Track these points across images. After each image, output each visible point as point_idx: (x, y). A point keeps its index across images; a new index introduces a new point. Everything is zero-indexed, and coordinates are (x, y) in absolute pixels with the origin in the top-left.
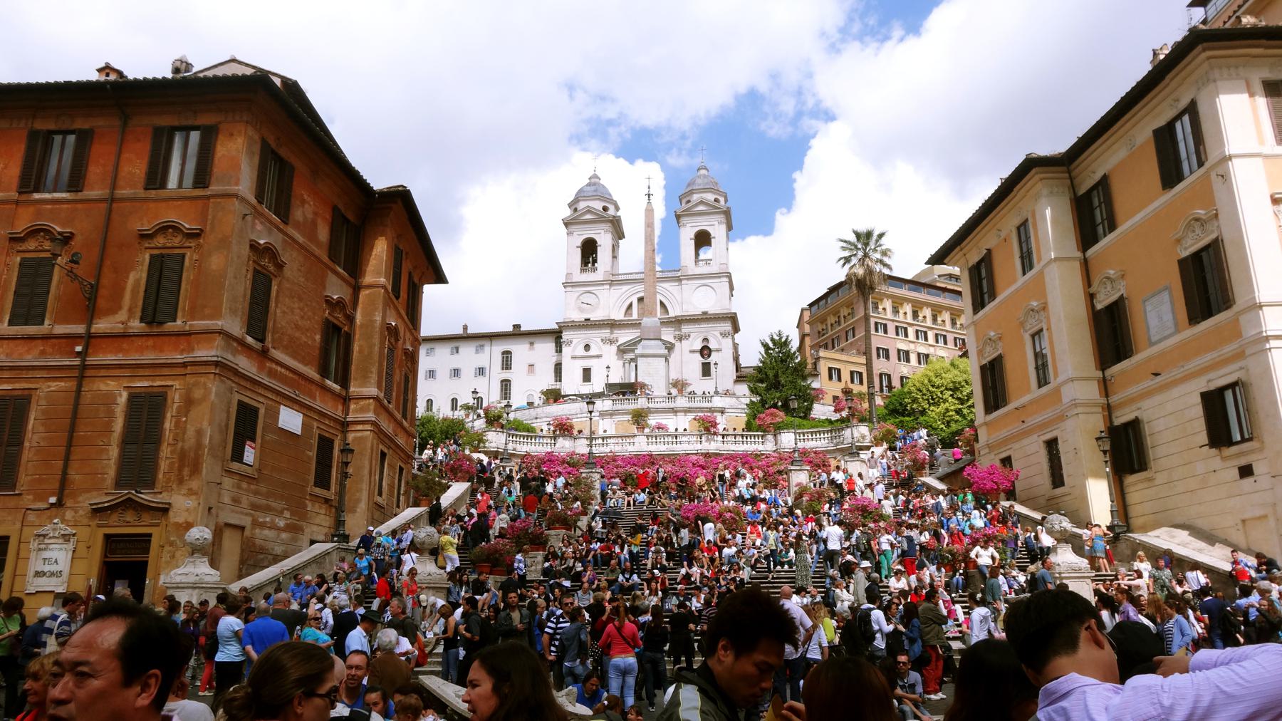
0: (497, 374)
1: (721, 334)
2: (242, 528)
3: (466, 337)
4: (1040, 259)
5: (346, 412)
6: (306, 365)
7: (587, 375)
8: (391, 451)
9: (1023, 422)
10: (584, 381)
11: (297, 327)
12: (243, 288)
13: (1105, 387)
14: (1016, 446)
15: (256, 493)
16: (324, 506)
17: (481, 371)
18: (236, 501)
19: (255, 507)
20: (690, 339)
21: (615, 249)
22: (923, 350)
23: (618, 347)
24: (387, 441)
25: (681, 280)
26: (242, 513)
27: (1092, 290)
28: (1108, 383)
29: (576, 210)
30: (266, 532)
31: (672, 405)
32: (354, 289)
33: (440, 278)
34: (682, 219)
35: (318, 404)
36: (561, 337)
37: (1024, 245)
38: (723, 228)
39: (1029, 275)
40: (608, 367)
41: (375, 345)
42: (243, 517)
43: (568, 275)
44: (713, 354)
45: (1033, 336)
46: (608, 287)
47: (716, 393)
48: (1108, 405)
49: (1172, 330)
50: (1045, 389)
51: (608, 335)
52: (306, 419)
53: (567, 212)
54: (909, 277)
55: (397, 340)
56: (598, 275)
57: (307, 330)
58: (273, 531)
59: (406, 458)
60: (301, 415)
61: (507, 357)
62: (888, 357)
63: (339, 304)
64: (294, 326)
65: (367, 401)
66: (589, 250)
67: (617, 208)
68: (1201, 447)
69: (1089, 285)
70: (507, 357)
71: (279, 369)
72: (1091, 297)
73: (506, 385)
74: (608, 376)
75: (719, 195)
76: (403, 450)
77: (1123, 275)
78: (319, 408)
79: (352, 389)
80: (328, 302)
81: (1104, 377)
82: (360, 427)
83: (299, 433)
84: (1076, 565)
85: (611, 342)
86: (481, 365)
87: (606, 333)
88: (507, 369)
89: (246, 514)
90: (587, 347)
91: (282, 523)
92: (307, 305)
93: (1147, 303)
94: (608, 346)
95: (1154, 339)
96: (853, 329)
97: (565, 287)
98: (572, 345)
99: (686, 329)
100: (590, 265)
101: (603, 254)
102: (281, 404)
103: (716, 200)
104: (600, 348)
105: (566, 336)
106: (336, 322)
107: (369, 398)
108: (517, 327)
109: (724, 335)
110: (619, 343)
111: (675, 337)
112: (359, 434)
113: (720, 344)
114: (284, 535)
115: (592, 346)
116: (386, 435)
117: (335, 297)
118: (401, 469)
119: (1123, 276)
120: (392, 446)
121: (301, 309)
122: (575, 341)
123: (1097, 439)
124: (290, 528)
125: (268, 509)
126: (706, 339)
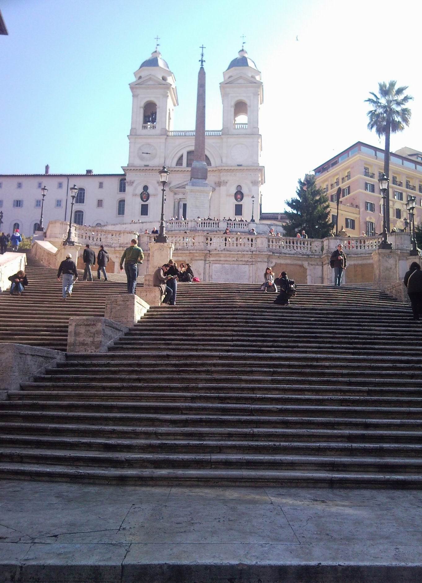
7: (144, 210)
10: (142, 214)
20: (228, 185)
23: (170, 188)
25: (222, 139)
29: (140, 78)
36: (125, 179)
43: (132, 130)
44: (244, 198)
53: (133, 79)
56: (157, 131)
70: (81, 193)
88: (80, 202)
90: (146, 188)
96: (349, 187)
97: (129, 139)
98: (134, 185)
104: (156, 189)
108: (89, 171)
113: (250, 191)
126: (239, 186)
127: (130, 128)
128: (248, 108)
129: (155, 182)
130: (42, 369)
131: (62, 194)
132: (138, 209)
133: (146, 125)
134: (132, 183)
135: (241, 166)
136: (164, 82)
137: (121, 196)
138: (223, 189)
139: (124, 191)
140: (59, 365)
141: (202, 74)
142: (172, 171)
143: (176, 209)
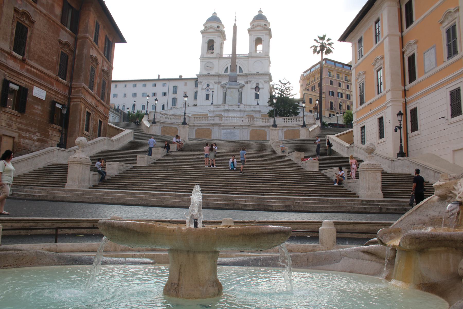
0: (171, 95)
1: (264, 81)
2: (14, 138)
3: (159, 80)
4: (382, 36)
5: (70, 92)
6: (48, 69)
8: (94, 113)
9: (371, 110)
10: (206, 99)
11: (43, 52)
12: (10, 29)
13: (405, 93)
14: (367, 121)
15: (20, 123)
16: (59, 133)
17: (165, 94)
18: (9, 125)
19: (19, 129)
20: (251, 83)
21: (222, 44)
22: (348, 93)
23: (221, 85)
24: (91, 108)
25: (249, 58)
26: (13, 131)
27: (403, 50)
28: (407, 92)
29: (206, 27)
30: (27, 141)
31: (239, 109)
32: (75, 39)
33: (122, 40)
34: (251, 32)
35: (55, 88)
36: (198, 81)
37: (377, 30)
38: (268, 37)
39: (378, 43)
40: (213, 92)
41: (83, 64)
42: (13, 133)
43: (202, 54)
45: (378, 71)
46: (218, 60)
47: (258, 104)
48: (406, 102)
49: (434, 66)
50: (380, 95)
51: (217, 80)
52: (47, 93)
53: (203, 28)
54: (346, 63)
55: (97, 64)
57: (48, 54)
58: (30, 141)
59: (103, 117)
60: (45, 92)
61: (175, 88)
62: (333, 95)
63: (67, 44)
64: (41, 51)
65: (79, 89)
66: (210, 45)
67: (224, 27)
68: (440, 118)
69: (403, 48)
70: (175, 88)
71: (33, 69)
72: (403, 53)
73: (174, 100)
74: (212, 96)
75: (267, 23)
76: (102, 114)
77: (417, 42)
78: (55, 90)
79: (73, 83)
80: (60, 42)
81: (405, 89)
82: (75, 100)
83: (44, 98)
84: (375, 165)
85: (218, 83)
86: (165, 92)
87: (216, 79)
89: (15, 132)
90: (208, 85)
91: (35, 138)
92: (49, 43)
93: (425, 54)
94: (216, 86)
95: (426, 71)
97: (200, 59)
98: (202, 84)
99: (249, 79)
100: (211, 51)
101: (216, 45)
102: (34, 85)
103: (265, 25)
105: (199, 80)
106: (65, 52)
107: (80, 87)
108: (181, 76)
109: (266, 82)
110: (221, 84)
111: (245, 82)
112: (75, 103)
114: (37, 143)
115: (210, 84)
116: (90, 105)
117: (64, 41)
118: (101, 122)
119: (416, 43)
120: (95, 110)
121: (46, 44)
122: (203, 82)
123: (398, 114)
124: (38, 140)
125: (28, 131)
126: (258, 84)
127: (201, 54)
128: (263, 42)
129: (213, 82)
130: (125, 169)
131: (165, 90)
132: (204, 97)
133: (208, 52)
134: (201, 83)
135: (258, 72)
136: (218, 29)
137: (195, 90)
138: (248, 86)
139: (197, 87)
140: (130, 169)
141: (235, 27)
142: (222, 76)
143: (224, 96)
